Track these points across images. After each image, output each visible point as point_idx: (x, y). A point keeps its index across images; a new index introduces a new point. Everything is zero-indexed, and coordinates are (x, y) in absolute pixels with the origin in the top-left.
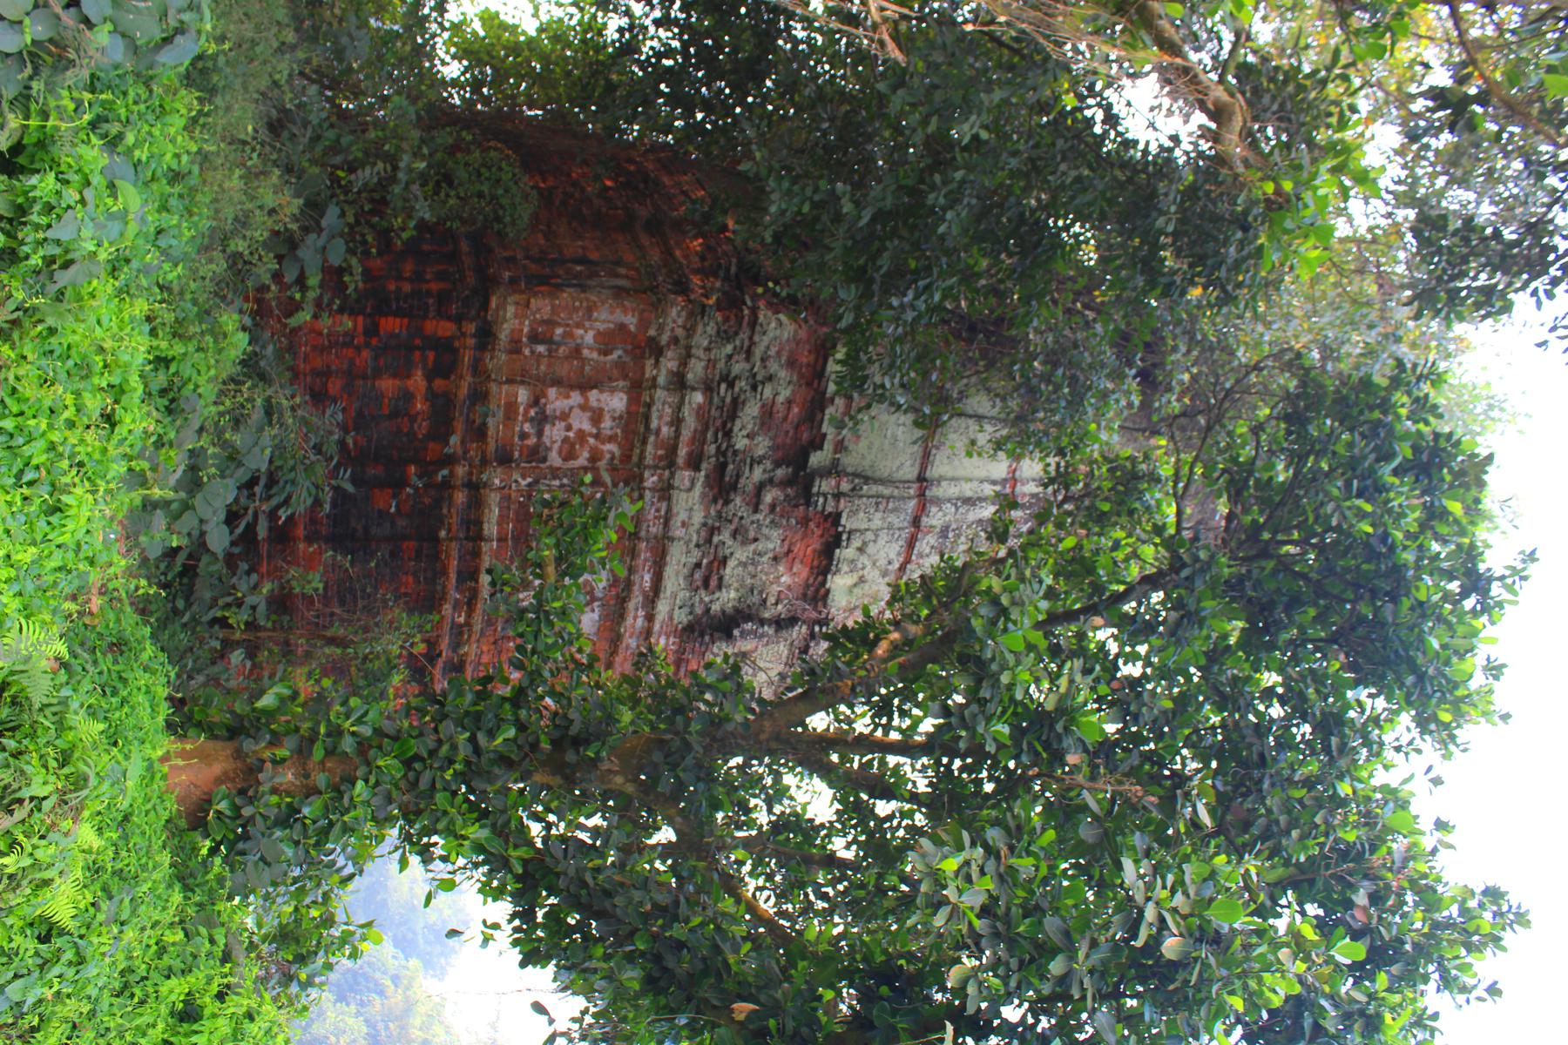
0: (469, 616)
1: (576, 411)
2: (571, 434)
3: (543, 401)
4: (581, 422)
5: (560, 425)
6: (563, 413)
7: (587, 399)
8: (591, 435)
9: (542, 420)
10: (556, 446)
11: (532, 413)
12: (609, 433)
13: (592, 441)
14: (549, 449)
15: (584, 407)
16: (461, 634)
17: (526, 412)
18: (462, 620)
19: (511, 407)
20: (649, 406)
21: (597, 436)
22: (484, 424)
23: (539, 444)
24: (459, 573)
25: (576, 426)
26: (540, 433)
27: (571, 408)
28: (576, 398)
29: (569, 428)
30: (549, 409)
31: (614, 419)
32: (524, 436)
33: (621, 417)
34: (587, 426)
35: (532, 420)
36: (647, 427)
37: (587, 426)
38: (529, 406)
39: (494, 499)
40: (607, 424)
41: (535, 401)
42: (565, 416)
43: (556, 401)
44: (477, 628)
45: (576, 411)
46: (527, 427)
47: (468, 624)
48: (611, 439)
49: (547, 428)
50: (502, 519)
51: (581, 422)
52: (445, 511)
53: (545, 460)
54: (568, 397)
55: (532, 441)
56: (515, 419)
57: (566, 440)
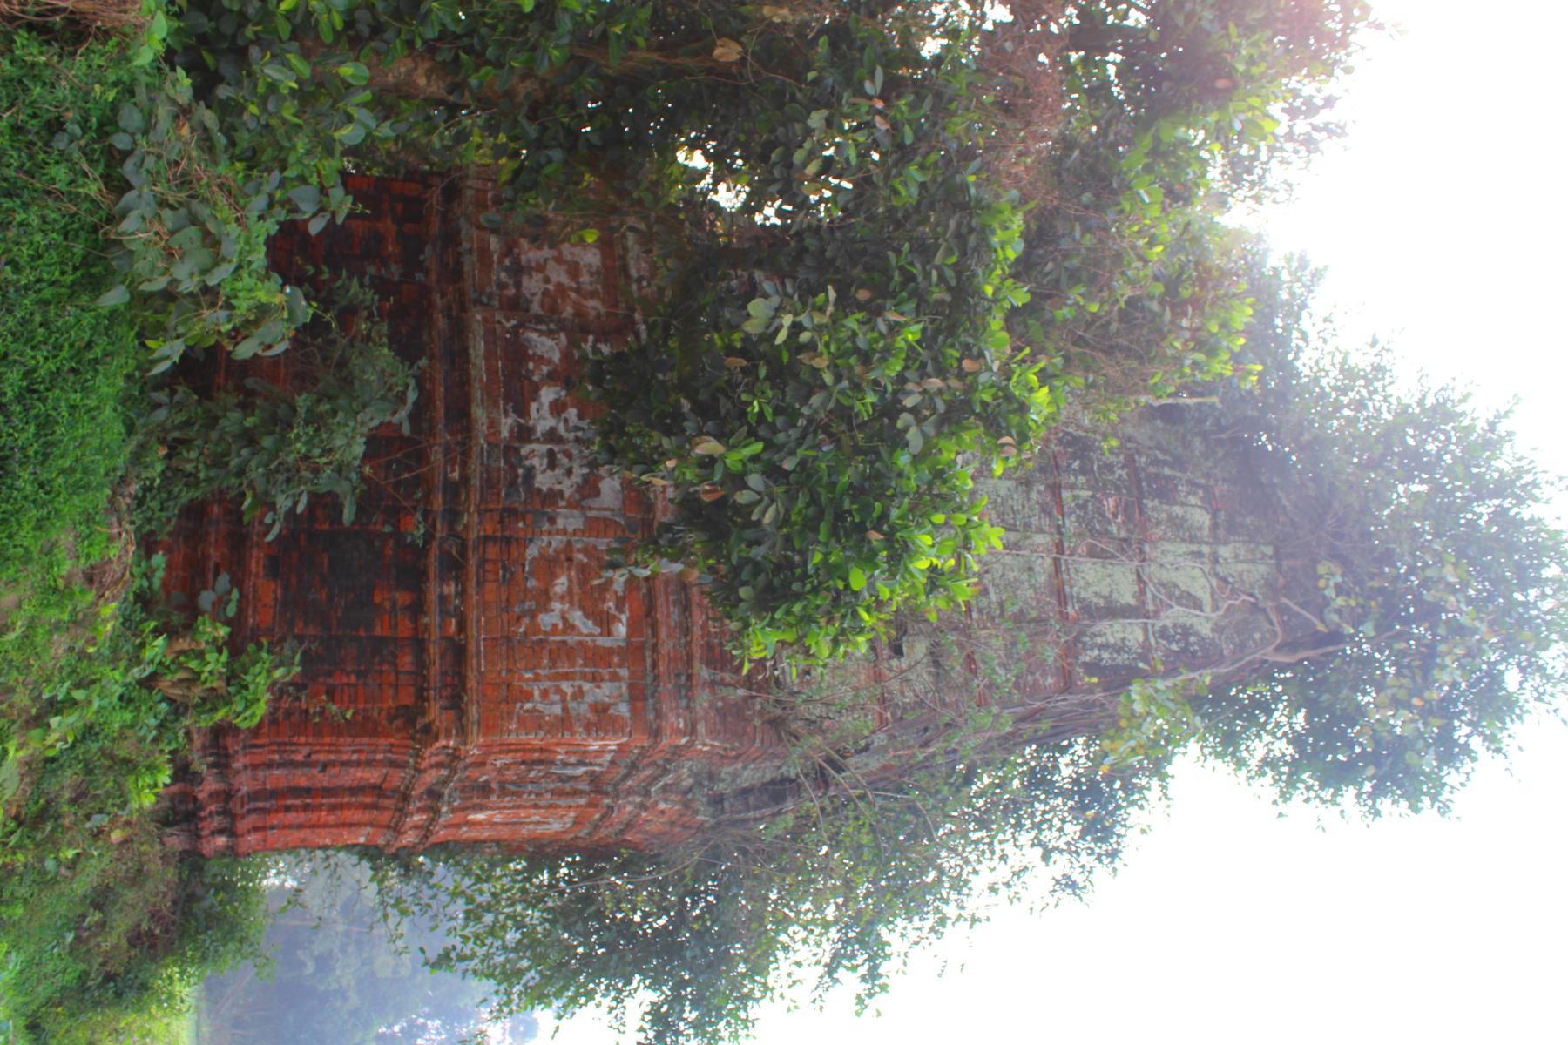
0: (464, 466)
1: (551, 264)
2: (551, 287)
3: (516, 251)
4: (559, 275)
5: (537, 277)
6: (538, 264)
7: (560, 253)
8: (571, 289)
9: (518, 271)
10: (537, 298)
11: (507, 262)
12: (589, 288)
13: (573, 295)
14: (529, 302)
15: (559, 260)
16: (457, 495)
17: (500, 262)
18: (456, 475)
19: (485, 252)
20: (623, 258)
21: (578, 291)
22: (459, 264)
23: (519, 295)
24: (447, 409)
25: (554, 278)
26: (518, 285)
27: (546, 260)
28: (546, 252)
29: (547, 280)
30: (523, 258)
31: (592, 275)
32: (502, 286)
33: (598, 273)
34: (565, 280)
35: (506, 269)
36: (627, 276)
37: (565, 280)
38: (503, 256)
39: (478, 349)
40: (585, 278)
41: (509, 249)
42: (540, 268)
43: (531, 254)
44: (476, 482)
45: (551, 264)
46: (503, 275)
47: (465, 479)
48: (593, 295)
49: (525, 281)
50: (489, 355)
51: (559, 275)
52: (425, 338)
53: (527, 310)
54: (540, 248)
55: (511, 291)
56: (490, 266)
57: (546, 293)
